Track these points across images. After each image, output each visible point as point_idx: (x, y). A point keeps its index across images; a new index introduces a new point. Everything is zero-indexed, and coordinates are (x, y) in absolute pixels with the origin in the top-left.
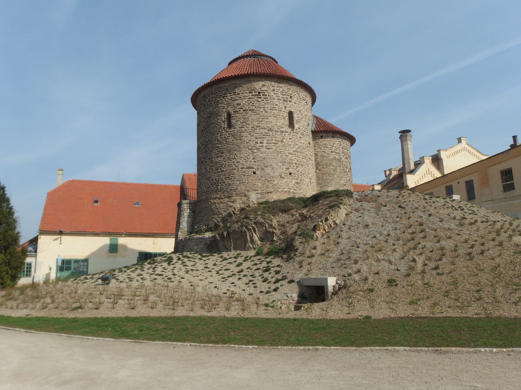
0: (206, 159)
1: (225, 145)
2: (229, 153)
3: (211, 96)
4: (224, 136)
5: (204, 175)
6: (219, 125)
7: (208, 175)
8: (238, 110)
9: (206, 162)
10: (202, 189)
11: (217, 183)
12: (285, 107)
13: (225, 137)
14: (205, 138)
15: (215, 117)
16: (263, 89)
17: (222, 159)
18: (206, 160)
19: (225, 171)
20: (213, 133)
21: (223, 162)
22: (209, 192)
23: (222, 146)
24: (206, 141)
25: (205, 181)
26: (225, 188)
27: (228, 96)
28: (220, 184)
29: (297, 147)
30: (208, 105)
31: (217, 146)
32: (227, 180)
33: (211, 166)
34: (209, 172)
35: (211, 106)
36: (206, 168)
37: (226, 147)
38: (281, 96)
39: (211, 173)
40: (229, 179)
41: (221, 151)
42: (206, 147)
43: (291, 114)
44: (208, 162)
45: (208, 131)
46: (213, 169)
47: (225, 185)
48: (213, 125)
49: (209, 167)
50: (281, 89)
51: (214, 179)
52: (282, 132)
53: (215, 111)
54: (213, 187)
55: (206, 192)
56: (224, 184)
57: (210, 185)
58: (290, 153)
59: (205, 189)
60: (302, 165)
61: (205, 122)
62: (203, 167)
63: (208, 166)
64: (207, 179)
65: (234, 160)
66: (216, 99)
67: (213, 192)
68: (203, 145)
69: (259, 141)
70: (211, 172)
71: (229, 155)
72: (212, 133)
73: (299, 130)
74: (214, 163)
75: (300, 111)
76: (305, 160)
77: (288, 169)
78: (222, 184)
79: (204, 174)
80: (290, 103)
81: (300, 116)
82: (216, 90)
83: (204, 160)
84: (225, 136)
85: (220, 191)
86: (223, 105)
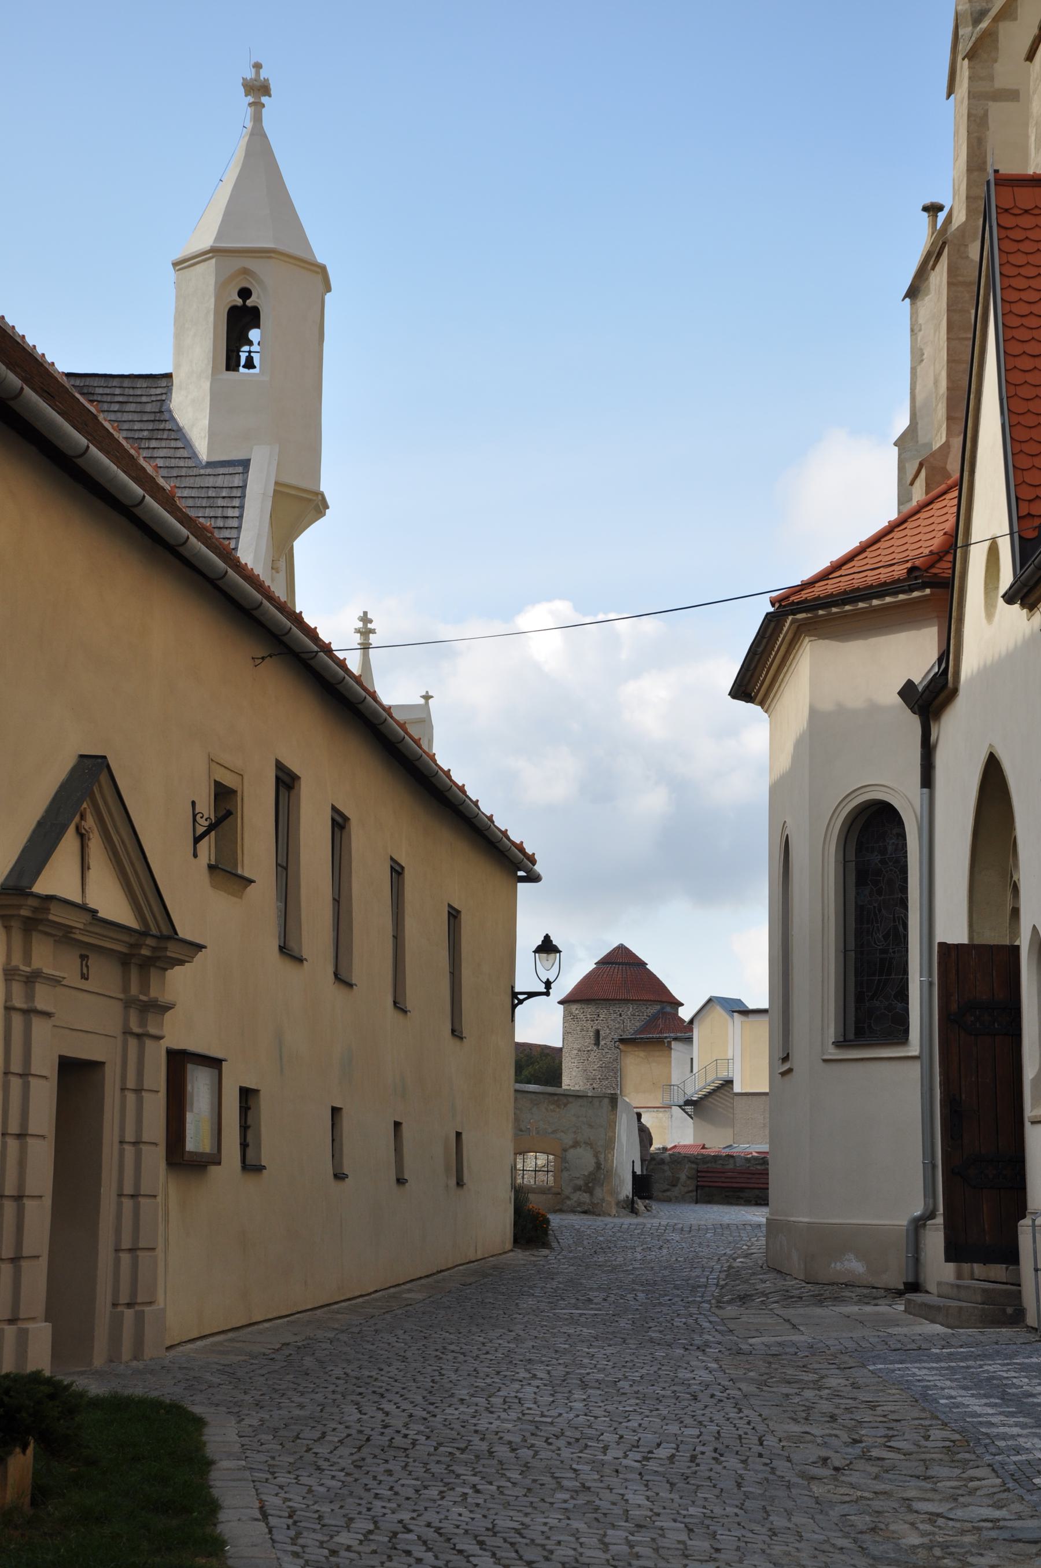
12: (592, 1027)
16: (577, 1012)
29: (601, 1063)
38: (589, 1016)
43: (597, 1033)
50: (590, 1010)
52: (588, 1051)
58: (594, 1070)
60: (608, 1078)
69: (573, 1061)
73: (605, 1046)
75: (608, 1027)
76: (611, 1074)
77: (592, 1084)
80: (597, 1022)
81: (608, 1031)
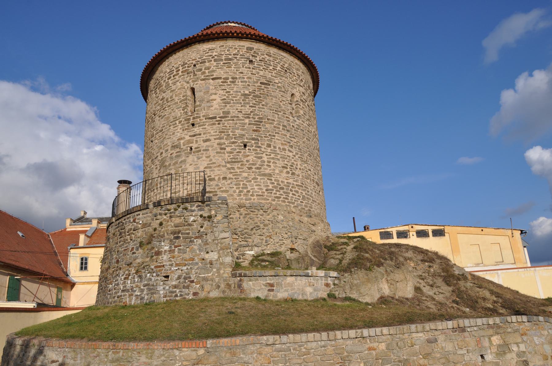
0: (260, 143)
1: (294, 138)
2: (300, 152)
3: (265, 56)
4: (291, 124)
5: (254, 167)
6: (283, 104)
7: (265, 169)
8: (304, 101)
9: (259, 147)
10: (247, 188)
11: (285, 187)
13: (293, 126)
14: (255, 110)
15: (276, 90)
17: (290, 154)
18: (260, 145)
19: (297, 175)
20: (276, 111)
21: (293, 160)
22: (270, 199)
23: (290, 137)
24: (257, 115)
25: (259, 177)
26: (299, 201)
27: (291, 74)
28: (291, 193)
30: (262, 66)
31: (283, 132)
32: (299, 189)
33: (273, 158)
34: (270, 166)
35: (267, 70)
36: (261, 157)
37: (295, 141)
39: (274, 170)
40: (302, 190)
41: (289, 143)
42: (260, 125)
44: (265, 148)
45: (263, 103)
46: (278, 165)
47: (299, 196)
48: (274, 99)
49: (268, 158)
51: (280, 180)
53: (277, 81)
54: (278, 193)
55: (262, 196)
56: (297, 195)
57: (270, 187)
59: (256, 190)
61: (254, 86)
62: (249, 152)
63: (264, 155)
64: (264, 175)
65: (306, 165)
66: (277, 67)
67: (279, 201)
68: (249, 118)
70: (272, 167)
71: (300, 155)
72: (273, 110)
74: (279, 157)
78: (293, 192)
79: (253, 164)
82: (275, 55)
83: (253, 142)
84: (294, 125)
85: (293, 203)
86: (288, 81)
